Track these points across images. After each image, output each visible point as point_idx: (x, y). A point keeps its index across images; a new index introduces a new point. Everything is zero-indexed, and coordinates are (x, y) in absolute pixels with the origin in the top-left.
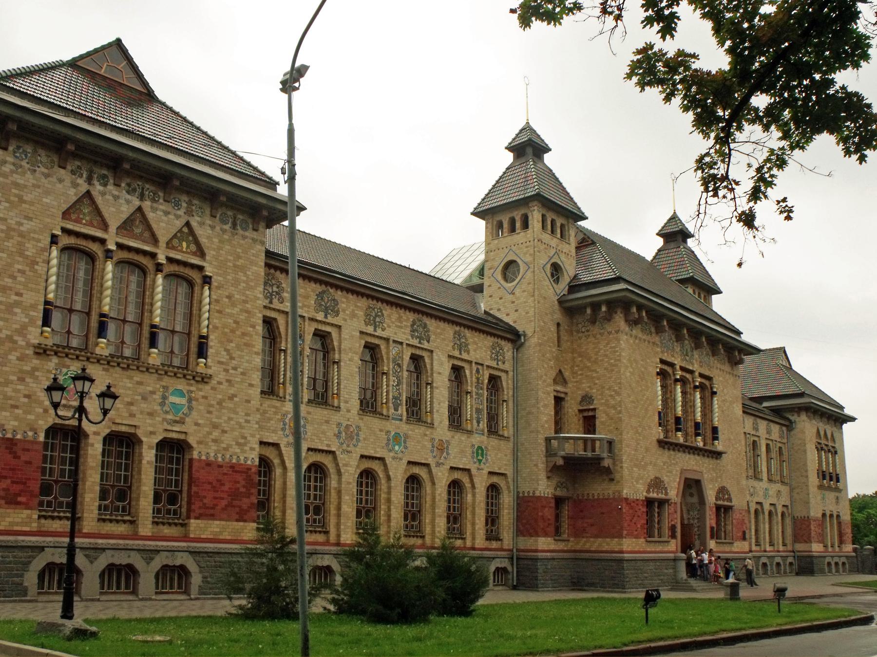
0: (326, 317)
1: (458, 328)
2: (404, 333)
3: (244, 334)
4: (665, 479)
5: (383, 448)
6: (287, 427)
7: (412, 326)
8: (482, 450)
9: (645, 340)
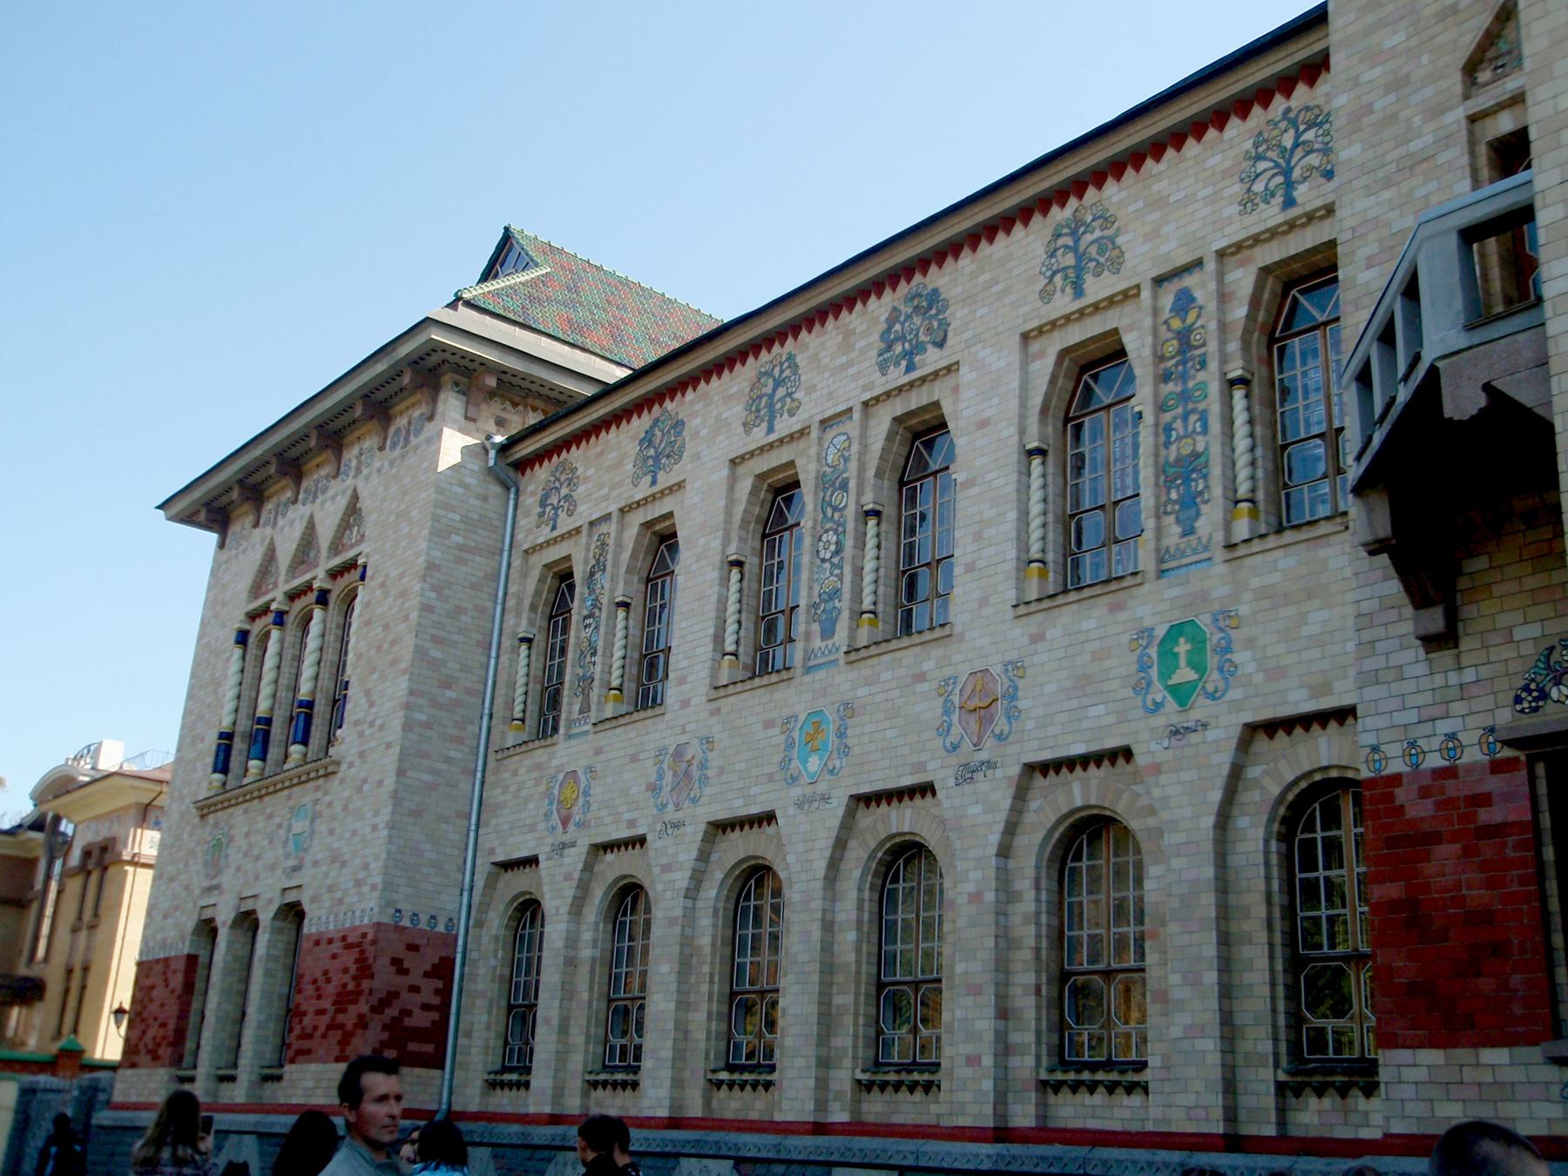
7: (884, 336)
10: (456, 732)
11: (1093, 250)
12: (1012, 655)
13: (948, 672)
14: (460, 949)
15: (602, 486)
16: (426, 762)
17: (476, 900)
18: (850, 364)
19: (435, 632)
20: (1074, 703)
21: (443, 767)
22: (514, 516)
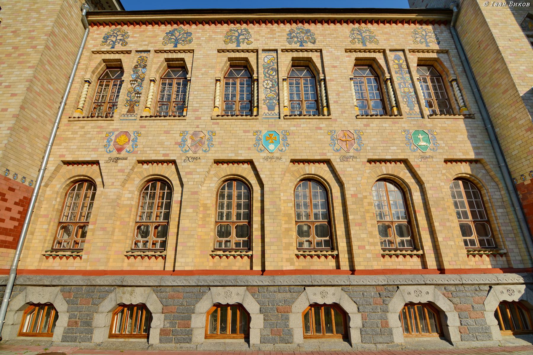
2: (278, 42)
3: (20, 55)
5: (249, 149)
6: (112, 143)
10: (50, 104)
11: (368, 38)
12: (359, 128)
13: (331, 129)
14: (35, 194)
15: (145, 41)
16: (34, 109)
17: (48, 174)
18: (274, 38)
19: (50, 59)
20: (385, 145)
21: (42, 115)
22: (86, 39)
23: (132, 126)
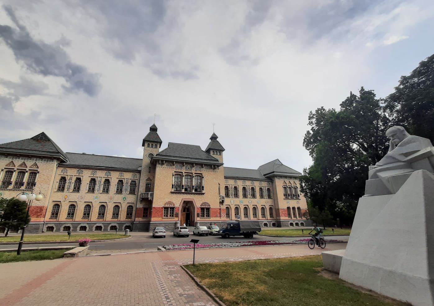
0: (79, 175)
1: (120, 172)
4: (174, 202)
8: (126, 198)
9: (168, 168)
23: (68, 194)
